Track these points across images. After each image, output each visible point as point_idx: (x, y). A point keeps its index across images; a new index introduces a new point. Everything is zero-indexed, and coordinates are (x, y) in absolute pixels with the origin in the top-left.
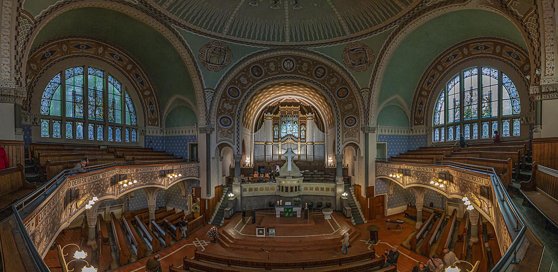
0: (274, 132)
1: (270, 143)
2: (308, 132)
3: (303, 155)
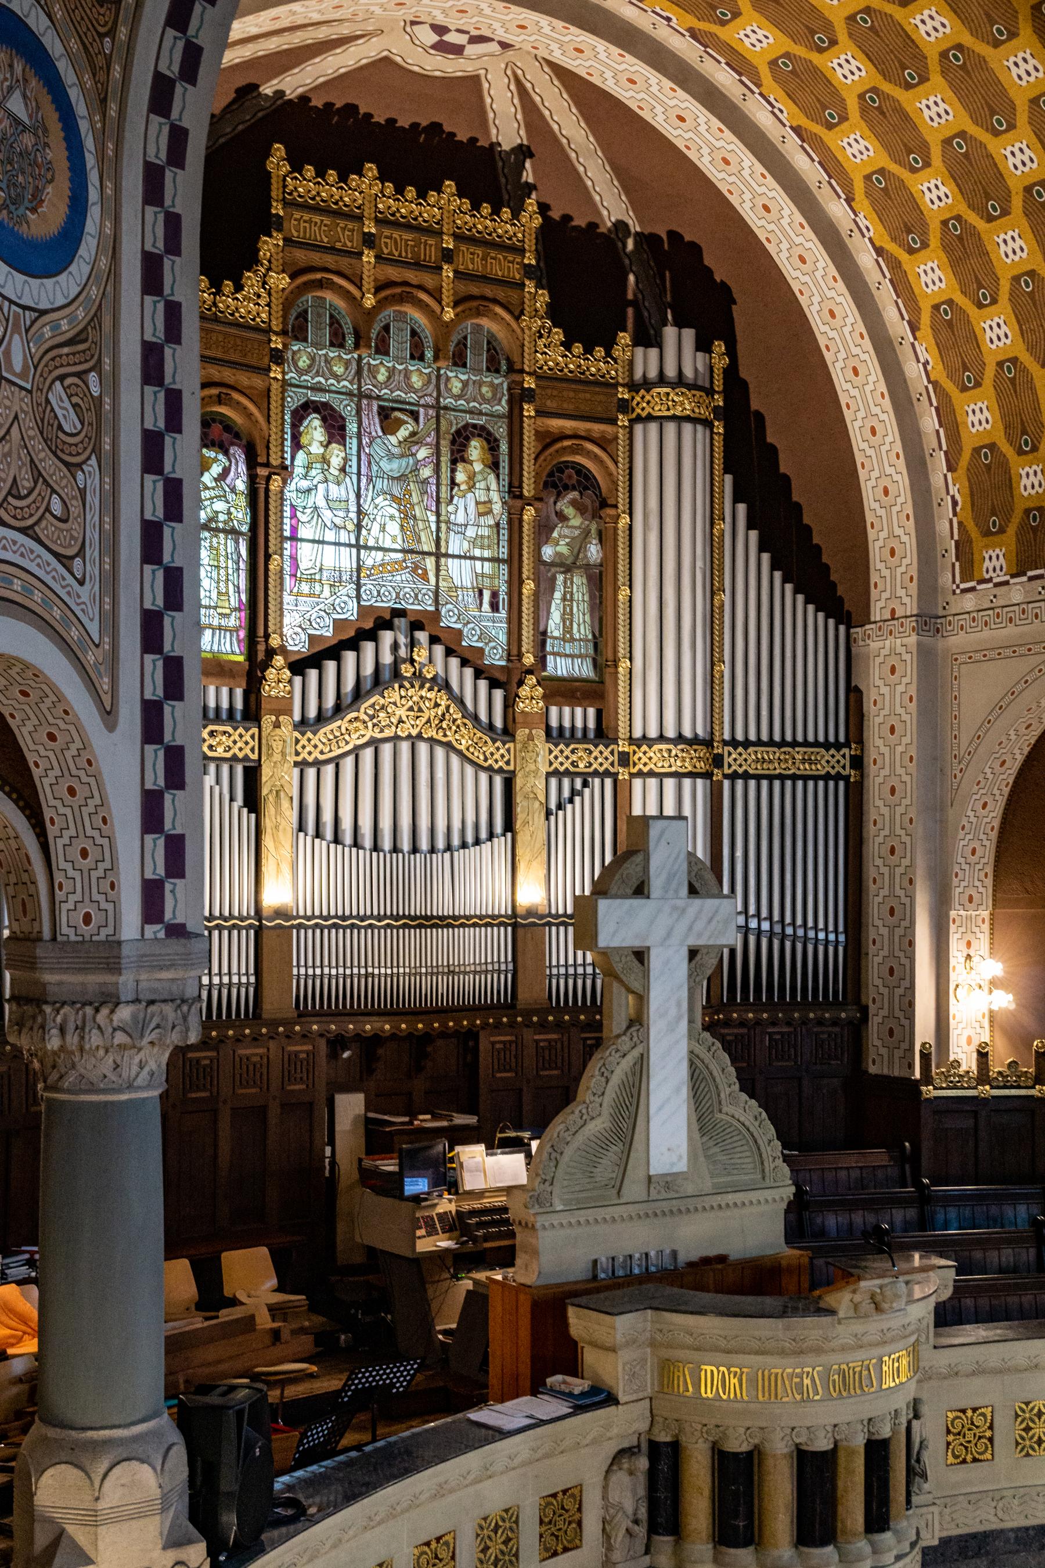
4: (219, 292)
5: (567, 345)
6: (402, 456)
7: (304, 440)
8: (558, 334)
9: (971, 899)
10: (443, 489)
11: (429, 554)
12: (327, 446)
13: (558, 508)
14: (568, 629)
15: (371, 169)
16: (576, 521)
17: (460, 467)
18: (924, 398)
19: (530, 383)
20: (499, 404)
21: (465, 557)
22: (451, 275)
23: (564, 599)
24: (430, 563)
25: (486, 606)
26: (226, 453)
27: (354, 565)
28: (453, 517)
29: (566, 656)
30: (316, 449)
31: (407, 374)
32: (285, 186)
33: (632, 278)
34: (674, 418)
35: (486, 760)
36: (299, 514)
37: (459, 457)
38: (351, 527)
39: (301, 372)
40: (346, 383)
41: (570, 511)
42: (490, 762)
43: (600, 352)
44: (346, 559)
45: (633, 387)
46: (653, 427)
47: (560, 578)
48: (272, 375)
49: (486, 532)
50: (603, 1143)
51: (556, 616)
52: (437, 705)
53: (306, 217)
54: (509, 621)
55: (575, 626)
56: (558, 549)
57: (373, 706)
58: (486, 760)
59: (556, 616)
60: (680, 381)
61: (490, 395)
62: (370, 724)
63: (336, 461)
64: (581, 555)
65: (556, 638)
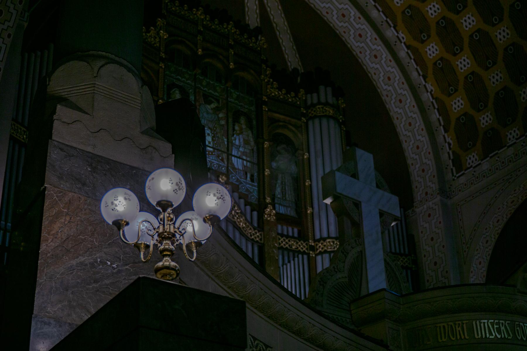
8: (275, 85)
17: (237, 124)
18: (432, 107)
24: (225, 156)
25: (248, 179)
28: (234, 141)
34: (325, 116)
35: (251, 236)
37: (236, 120)
42: (253, 237)
43: (293, 94)
46: (317, 121)
54: (259, 186)
58: (251, 236)
60: (327, 104)
65: (279, 198)
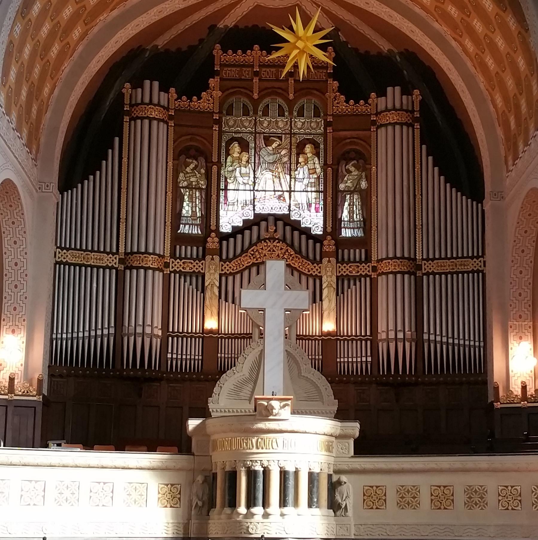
0: (178, 200)
1: (151, 261)
2: (381, 202)
3: (350, 339)
4: (191, 101)
5: (347, 102)
6: (274, 154)
7: (230, 152)
9: (520, 317)
10: (293, 165)
11: (287, 191)
12: (240, 153)
13: (347, 168)
14: (351, 217)
15: (256, 47)
16: (356, 173)
17: (301, 156)
19: (330, 119)
20: (320, 129)
21: (303, 191)
22: (293, 82)
23: (349, 205)
24: (286, 195)
26: (196, 160)
27: (252, 198)
28: (297, 176)
29: (350, 228)
30: (236, 155)
31: (277, 122)
32: (220, 59)
33: (405, 72)
35: (309, 271)
36: (228, 180)
37: (300, 150)
38: (251, 183)
39: (230, 127)
40: (250, 129)
41: (352, 169)
42: (311, 272)
44: (248, 196)
45: (377, 114)
47: (348, 197)
48: (214, 129)
49: (313, 180)
50: (245, 382)
51: (345, 213)
52: (281, 249)
53: (229, 69)
55: (355, 216)
56: (347, 184)
57: (253, 250)
58: (309, 271)
59: (345, 213)
61: (315, 126)
62: (252, 258)
63: (245, 158)
64: (358, 186)
